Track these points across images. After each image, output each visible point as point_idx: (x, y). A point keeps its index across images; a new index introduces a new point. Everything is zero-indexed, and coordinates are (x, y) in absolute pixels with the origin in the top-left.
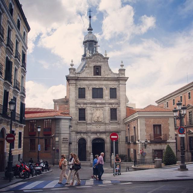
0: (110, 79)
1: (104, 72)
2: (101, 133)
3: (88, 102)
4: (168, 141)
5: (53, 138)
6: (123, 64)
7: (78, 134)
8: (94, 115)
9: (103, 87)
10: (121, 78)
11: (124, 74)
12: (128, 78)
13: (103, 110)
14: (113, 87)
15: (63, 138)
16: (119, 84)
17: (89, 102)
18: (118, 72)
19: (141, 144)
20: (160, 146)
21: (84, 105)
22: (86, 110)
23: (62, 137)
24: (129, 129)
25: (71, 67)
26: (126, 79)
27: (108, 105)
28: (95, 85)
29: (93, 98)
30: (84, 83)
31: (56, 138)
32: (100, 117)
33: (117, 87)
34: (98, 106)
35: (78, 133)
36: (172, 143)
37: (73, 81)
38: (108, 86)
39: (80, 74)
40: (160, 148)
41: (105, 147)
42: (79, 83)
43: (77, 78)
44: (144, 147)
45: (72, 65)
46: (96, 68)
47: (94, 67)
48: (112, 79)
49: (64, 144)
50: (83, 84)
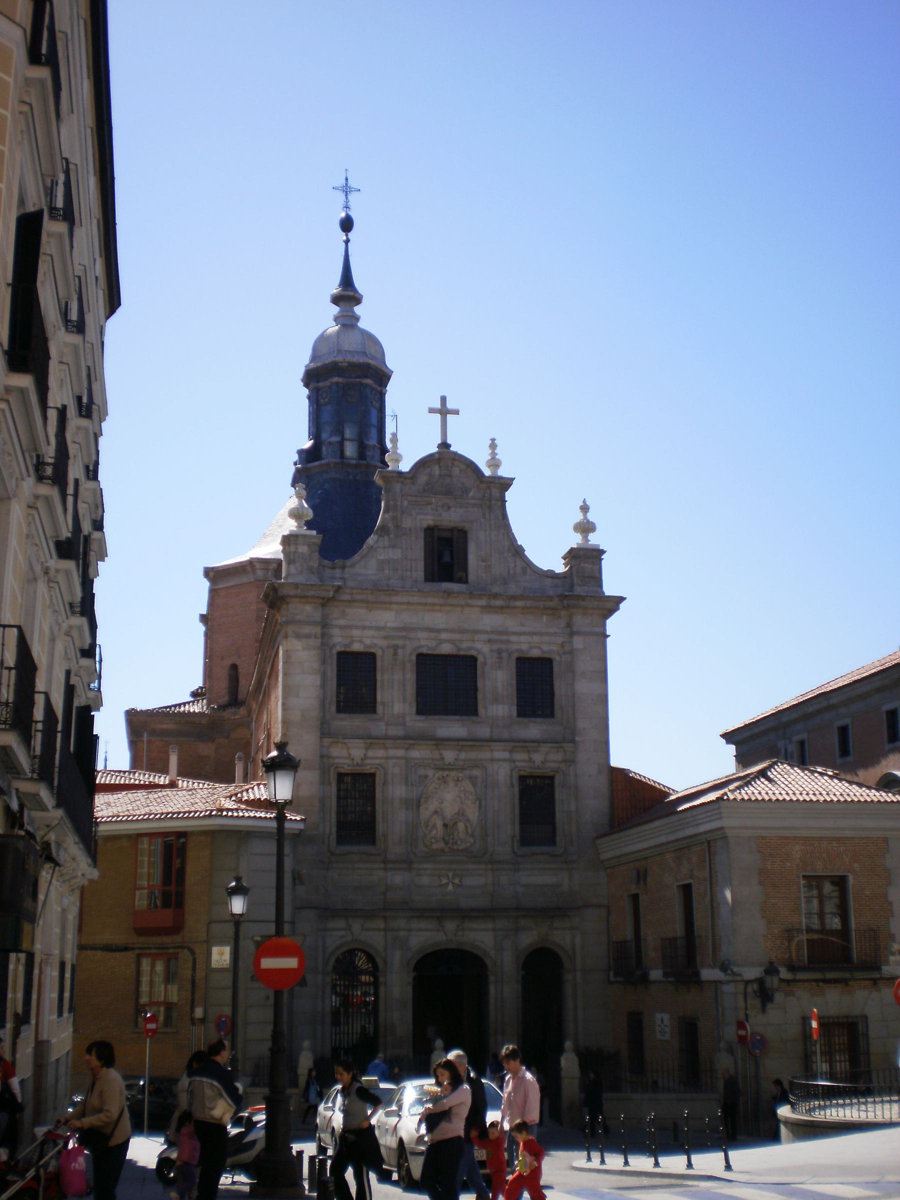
0: (519, 603)
1: (484, 561)
2: (465, 914)
3: (393, 731)
5: (192, 952)
7: (332, 924)
8: (426, 812)
9: (478, 645)
10: (583, 598)
11: (598, 580)
12: (622, 599)
13: (474, 785)
14: (535, 653)
17: (400, 732)
18: (560, 568)
19: (741, 987)
21: (371, 753)
22: (379, 779)
24: (635, 898)
26: (609, 605)
27: (506, 755)
28: (433, 635)
29: (419, 712)
30: (367, 624)
31: (215, 950)
32: (461, 826)
33: (554, 648)
34: (449, 755)
35: (327, 912)
37: (309, 608)
38: (508, 642)
41: (492, 1001)
42: (342, 622)
43: (331, 594)
44: (757, 1003)
46: (440, 539)
47: (430, 531)
50: (364, 628)
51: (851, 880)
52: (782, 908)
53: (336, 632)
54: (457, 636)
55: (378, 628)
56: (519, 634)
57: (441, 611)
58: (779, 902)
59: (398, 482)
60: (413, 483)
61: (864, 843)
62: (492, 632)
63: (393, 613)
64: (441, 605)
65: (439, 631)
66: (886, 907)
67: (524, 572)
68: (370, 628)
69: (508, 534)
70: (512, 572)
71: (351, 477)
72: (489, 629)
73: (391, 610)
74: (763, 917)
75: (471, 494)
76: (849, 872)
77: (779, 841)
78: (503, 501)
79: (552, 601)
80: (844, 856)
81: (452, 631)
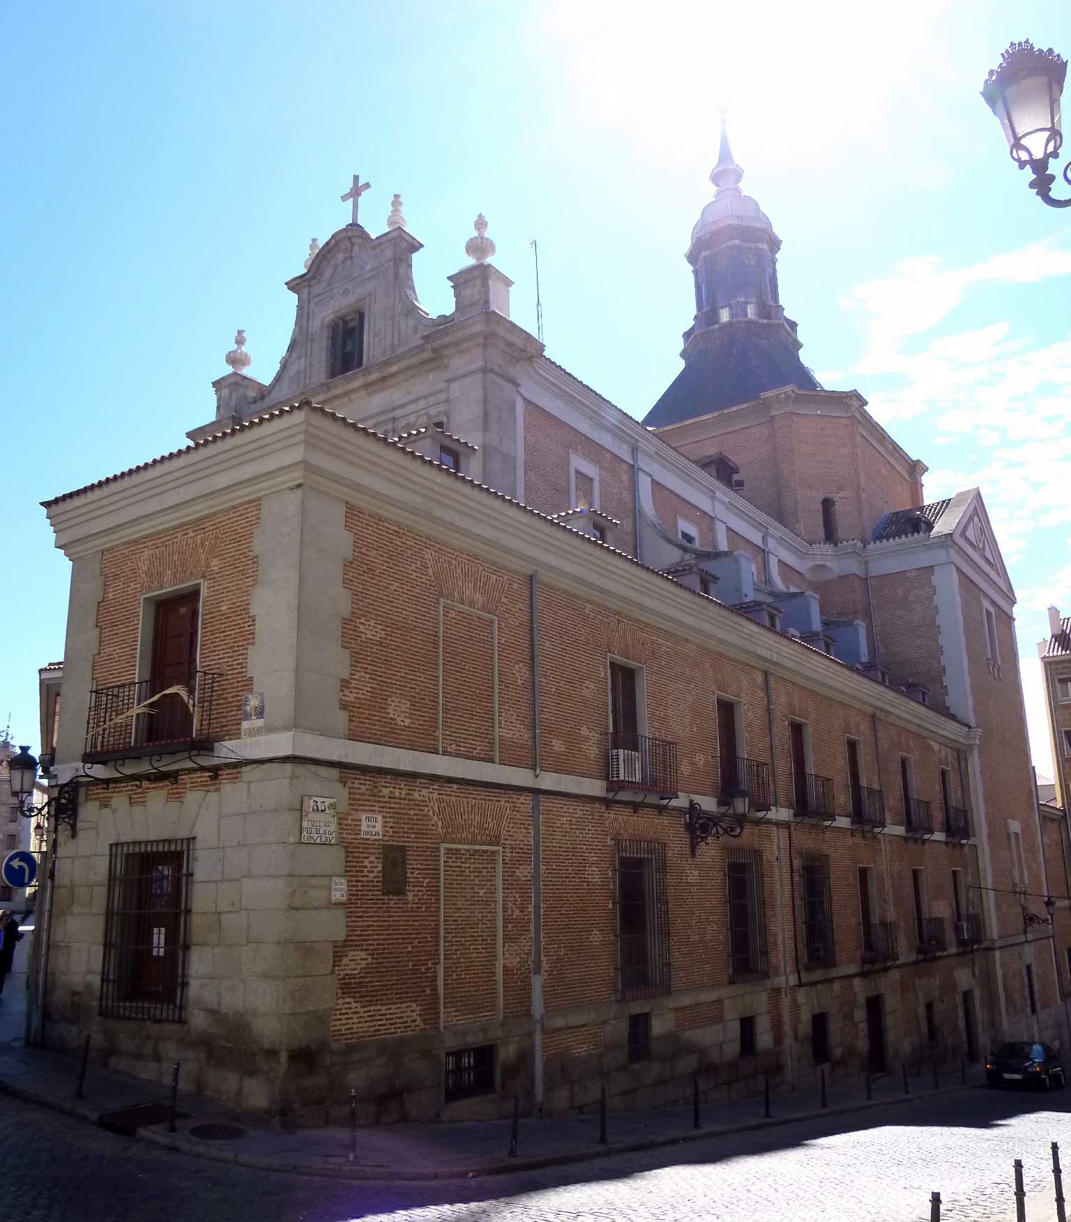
0: (394, 368)
16: (448, 389)
20: (174, 806)
33: (442, 408)
38: (394, 419)
45: (233, 359)
48: (403, 364)
56: (404, 405)
59: (305, 287)
60: (319, 282)
61: (229, 519)
62: (377, 414)
72: (376, 411)
75: (368, 267)
79: (423, 351)
80: (200, 551)
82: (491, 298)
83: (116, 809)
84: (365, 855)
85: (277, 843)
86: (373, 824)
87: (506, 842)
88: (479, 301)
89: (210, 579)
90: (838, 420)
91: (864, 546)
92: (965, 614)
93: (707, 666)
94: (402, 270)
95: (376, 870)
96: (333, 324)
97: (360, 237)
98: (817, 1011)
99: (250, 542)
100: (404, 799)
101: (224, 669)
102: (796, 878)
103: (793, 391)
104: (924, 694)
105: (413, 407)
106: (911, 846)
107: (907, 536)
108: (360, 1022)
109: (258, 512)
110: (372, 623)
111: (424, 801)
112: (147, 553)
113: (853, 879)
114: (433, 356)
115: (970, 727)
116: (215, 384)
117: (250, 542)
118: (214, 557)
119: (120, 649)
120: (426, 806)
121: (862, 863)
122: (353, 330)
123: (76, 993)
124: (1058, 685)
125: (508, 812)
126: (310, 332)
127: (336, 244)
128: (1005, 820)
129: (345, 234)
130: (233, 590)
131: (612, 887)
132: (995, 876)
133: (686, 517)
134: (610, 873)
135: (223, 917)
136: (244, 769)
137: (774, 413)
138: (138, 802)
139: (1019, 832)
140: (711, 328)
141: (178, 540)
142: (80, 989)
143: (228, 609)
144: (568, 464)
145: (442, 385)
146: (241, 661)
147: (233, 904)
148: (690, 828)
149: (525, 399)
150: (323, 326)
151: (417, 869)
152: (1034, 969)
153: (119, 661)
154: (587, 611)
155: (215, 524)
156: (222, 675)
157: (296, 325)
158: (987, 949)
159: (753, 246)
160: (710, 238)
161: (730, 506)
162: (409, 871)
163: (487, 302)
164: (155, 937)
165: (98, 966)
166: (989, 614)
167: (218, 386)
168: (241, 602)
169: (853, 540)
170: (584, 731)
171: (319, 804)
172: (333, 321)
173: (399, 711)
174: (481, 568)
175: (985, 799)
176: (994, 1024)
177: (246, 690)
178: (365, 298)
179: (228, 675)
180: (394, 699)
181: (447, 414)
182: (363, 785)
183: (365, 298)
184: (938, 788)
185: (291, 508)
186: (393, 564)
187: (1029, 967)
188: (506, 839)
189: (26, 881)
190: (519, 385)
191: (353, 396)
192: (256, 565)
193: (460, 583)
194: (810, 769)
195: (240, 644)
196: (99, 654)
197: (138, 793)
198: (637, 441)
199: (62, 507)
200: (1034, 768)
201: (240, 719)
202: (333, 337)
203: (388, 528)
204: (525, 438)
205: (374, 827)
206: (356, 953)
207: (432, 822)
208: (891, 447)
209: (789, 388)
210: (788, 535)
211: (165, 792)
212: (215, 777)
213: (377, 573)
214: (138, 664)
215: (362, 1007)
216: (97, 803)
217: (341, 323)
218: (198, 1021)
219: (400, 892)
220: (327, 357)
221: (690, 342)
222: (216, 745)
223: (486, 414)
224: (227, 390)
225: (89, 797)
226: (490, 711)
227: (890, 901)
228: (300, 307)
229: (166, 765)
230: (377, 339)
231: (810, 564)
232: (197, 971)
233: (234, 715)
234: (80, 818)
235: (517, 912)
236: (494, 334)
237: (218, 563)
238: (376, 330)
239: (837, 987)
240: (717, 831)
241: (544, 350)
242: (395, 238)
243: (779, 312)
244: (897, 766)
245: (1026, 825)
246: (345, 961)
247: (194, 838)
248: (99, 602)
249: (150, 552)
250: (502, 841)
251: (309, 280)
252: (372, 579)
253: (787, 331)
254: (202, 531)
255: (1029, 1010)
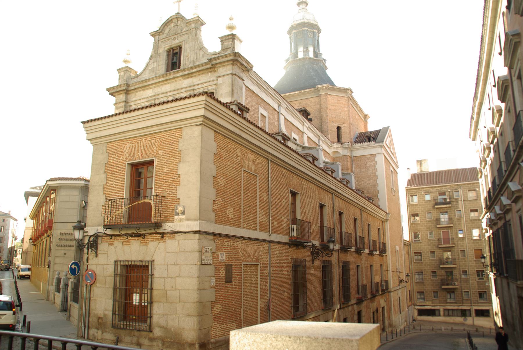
0: (194, 70)
4: (168, 227)
6: (234, 23)
15: (62, 234)
16: (217, 80)
20: (143, 248)
23: (59, 231)
25: (124, 65)
28: (165, 95)
30: (143, 97)
33: (214, 87)
36: (182, 236)
38: (194, 90)
39: (139, 77)
40: (140, 259)
43: (125, 88)
47: (169, 51)
48: (199, 69)
49: (63, 248)
51: (156, 163)
52: (114, 187)
53: (132, 103)
54: (174, 93)
55: (145, 98)
56: (198, 85)
57: (168, 83)
58: (113, 183)
59: (157, 35)
60: (163, 34)
61: (167, 135)
63: (152, 89)
64: (167, 80)
65: (167, 93)
66: (176, 179)
67: (203, 56)
68: (143, 99)
69: (197, 41)
70: (198, 58)
71: (298, 65)
72: (186, 86)
73: (150, 88)
74: (103, 194)
76: (154, 157)
77: (118, 144)
78: (197, 29)
79: (208, 64)
81: (171, 91)
82: (236, 47)
83: (116, 247)
84: (220, 268)
85: (192, 264)
86: (223, 256)
87: (261, 261)
88: (230, 47)
89: (158, 158)
90: (343, 98)
91: (352, 145)
92: (386, 172)
93: (317, 192)
94: (198, 32)
95: (223, 274)
96: (168, 50)
97: (181, 18)
98: (345, 317)
99: (177, 145)
100: (232, 246)
101: (166, 194)
102: (340, 270)
103: (328, 86)
104: (373, 200)
105: (202, 86)
106: (370, 257)
107: (363, 143)
108: (219, 331)
109: (181, 133)
110: (222, 178)
111: (237, 247)
112: (128, 145)
113: (355, 269)
114: (212, 66)
115: (386, 213)
116: (118, 70)
117: (177, 145)
118: (160, 149)
119: (116, 183)
120: (238, 248)
121: (357, 263)
122: (177, 53)
123: (99, 318)
124: (410, 197)
125: (262, 250)
126: (159, 53)
127: (171, 20)
128: (395, 246)
129: (175, 17)
130: (169, 163)
131: (290, 276)
132: (392, 266)
133: (295, 132)
134: (290, 271)
135: (168, 292)
136: (176, 235)
137: (320, 93)
138: (126, 245)
139: (398, 250)
140: (296, 59)
141: (143, 141)
142: (102, 316)
143: (167, 170)
144: (258, 111)
145: (215, 78)
146: (173, 192)
147: (172, 287)
148: (312, 253)
149: (245, 86)
150: (164, 51)
151: (236, 273)
152: (401, 298)
153: (115, 187)
154: (284, 172)
155: (160, 136)
156: (165, 197)
157: (153, 49)
158: (389, 292)
159: (312, 30)
160: (297, 26)
161: (309, 128)
162: (233, 273)
163: (234, 48)
164: (134, 298)
165: (110, 307)
166: (392, 171)
167: (119, 71)
168: (173, 168)
169: (348, 142)
170: (283, 218)
171: (207, 249)
172: (168, 49)
173: (230, 213)
174: (254, 156)
175: (390, 239)
176: (390, 318)
177: (176, 203)
178: (183, 42)
179: (168, 197)
180: (228, 208)
181: (216, 90)
182: (219, 241)
183: (183, 42)
184: (377, 235)
185: (196, 133)
186: (229, 155)
187: (399, 297)
188: (261, 260)
189: (77, 273)
190: (244, 80)
191: (177, 79)
192: (180, 154)
193: (248, 162)
194: (344, 230)
195: (173, 185)
196: (106, 184)
197: (126, 241)
198: (280, 103)
199: (90, 124)
200: (402, 227)
201: (173, 215)
202: (168, 55)
203: (227, 141)
204: (245, 100)
205: (223, 257)
206: (218, 305)
207: (240, 255)
208: (359, 108)
209: (326, 85)
210: (326, 141)
211: (139, 241)
212: (163, 237)
213: (223, 159)
214: (125, 189)
215: (220, 326)
216: (107, 244)
217: (172, 50)
218: (157, 332)
219: (231, 282)
220: (165, 63)
221: (288, 64)
222: (163, 224)
223: (233, 90)
224: (123, 72)
225: (103, 241)
226: (256, 212)
227: (364, 277)
228: (155, 43)
229: (141, 232)
230: (187, 58)
231: (333, 150)
232: (156, 312)
233: (170, 213)
234: (99, 249)
235: (264, 287)
236: (237, 61)
237: (162, 152)
238: (187, 54)
239: (350, 308)
240: (322, 255)
241: (253, 68)
242: (197, 20)
243: (321, 56)
244: (366, 227)
245: (400, 247)
246: (215, 309)
247: (154, 261)
248: (106, 163)
249: (130, 145)
250: (260, 261)
251: (159, 33)
252: (222, 161)
253: (323, 63)
254: (154, 139)
255: (399, 312)
